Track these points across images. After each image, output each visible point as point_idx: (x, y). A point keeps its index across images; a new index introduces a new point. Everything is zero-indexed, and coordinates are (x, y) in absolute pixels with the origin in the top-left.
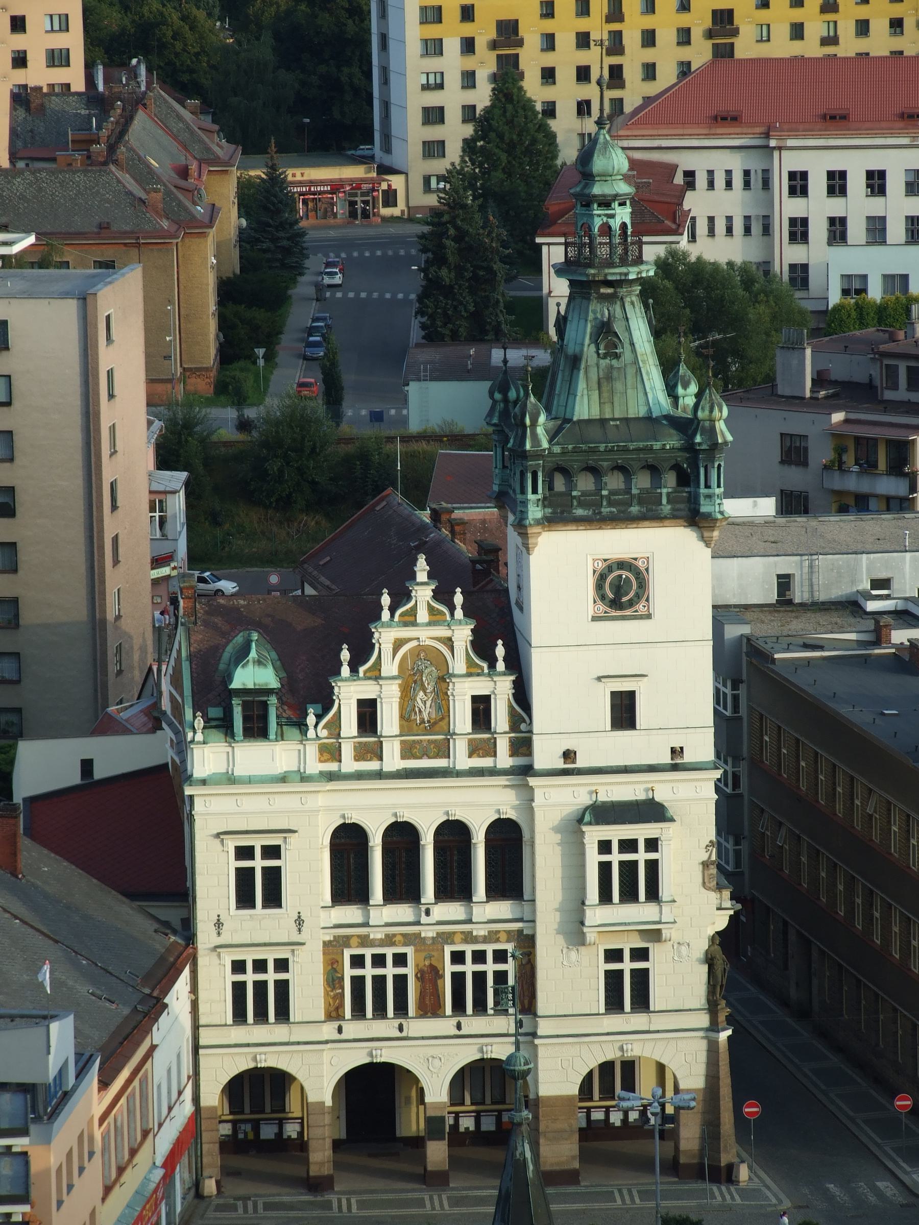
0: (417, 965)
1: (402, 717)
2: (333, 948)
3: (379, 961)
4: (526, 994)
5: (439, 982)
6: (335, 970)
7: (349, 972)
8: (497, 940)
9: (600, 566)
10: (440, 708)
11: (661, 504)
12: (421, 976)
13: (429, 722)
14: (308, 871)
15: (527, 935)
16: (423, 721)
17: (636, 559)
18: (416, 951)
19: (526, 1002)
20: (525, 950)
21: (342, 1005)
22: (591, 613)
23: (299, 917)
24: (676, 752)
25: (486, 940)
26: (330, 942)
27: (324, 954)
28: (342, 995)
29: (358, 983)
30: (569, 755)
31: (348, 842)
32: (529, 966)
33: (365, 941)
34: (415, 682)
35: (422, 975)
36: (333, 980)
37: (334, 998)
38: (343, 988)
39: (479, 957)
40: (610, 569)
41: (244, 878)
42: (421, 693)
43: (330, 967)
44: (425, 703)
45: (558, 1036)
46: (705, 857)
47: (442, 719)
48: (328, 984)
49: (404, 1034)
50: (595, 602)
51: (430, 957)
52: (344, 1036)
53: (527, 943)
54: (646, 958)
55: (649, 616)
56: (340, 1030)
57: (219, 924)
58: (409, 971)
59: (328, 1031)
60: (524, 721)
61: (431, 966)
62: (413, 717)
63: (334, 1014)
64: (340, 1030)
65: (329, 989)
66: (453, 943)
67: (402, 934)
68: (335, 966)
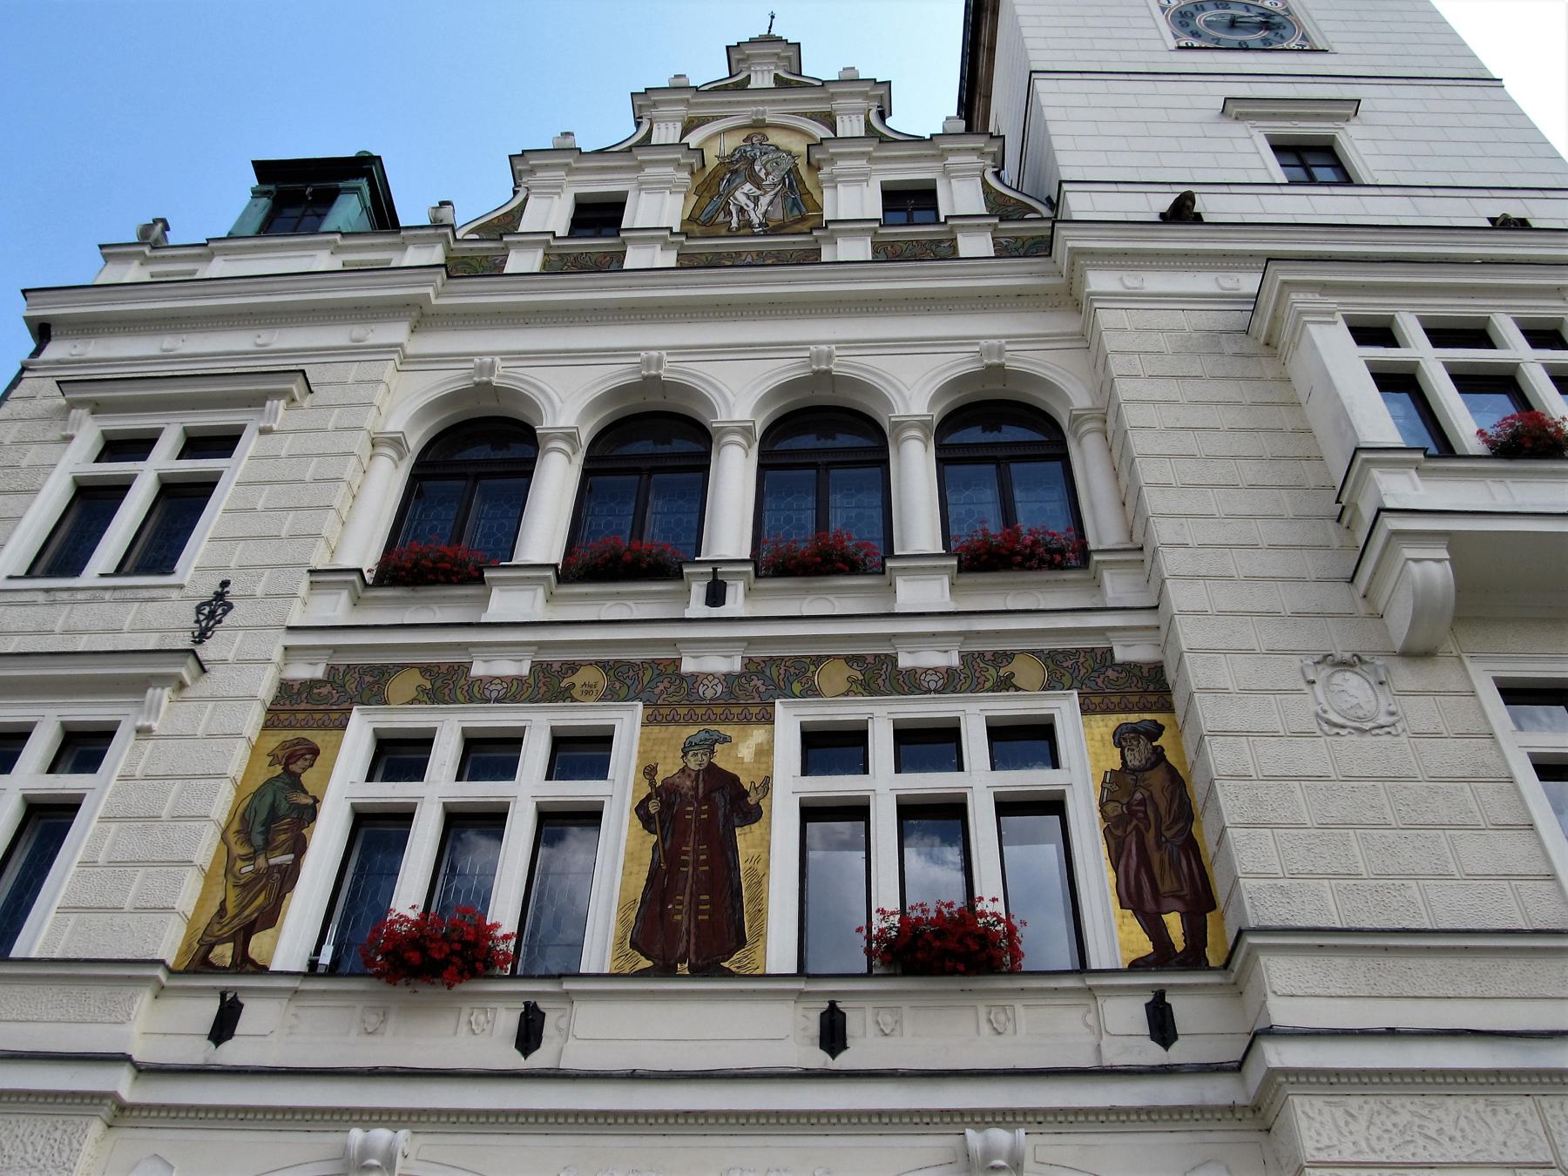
0: (650, 772)
1: (691, 219)
3: (490, 755)
4: (1167, 885)
5: (745, 840)
6: (293, 781)
7: (345, 781)
8: (1006, 684)
10: (795, 204)
12: (662, 810)
13: (761, 225)
14: (316, 496)
15: (1129, 668)
16: (749, 224)
18: (648, 722)
19: (1174, 923)
20: (1133, 718)
21: (270, 917)
22: (1172, 44)
23: (220, 596)
25: (950, 681)
26: (312, 684)
27: (268, 726)
28: (289, 876)
29: (379, 833)
31: (474, 457)
32: (1157, 778)
33: (446, 683)
34: (735, 172)
35: (666, 805)
36: (272, 821)
37: (246, 887)
38: (299, 847)
39: (928, 744)
41: (93, 503)
42: (748, 187)
43: (279, 769)
44: (756, 200)
45: (1391, 1033)
47: (803, 219)
48: (245, 833)
49: (539, 1060)
50: (1176, 37)
51: (710, 743)
52: (232, 1053)
53: (1141, 694)
56: (223, 1028)
58: (616, 793)
59: (169, 1026)
60: (1035, 211)
61: (712, 770)
62: (721, 218)
63: (224, 953)
64: (223, 1028)
65: (240, 850)
66: (812, 691)
67: (603, 665)
68: (293, 768)
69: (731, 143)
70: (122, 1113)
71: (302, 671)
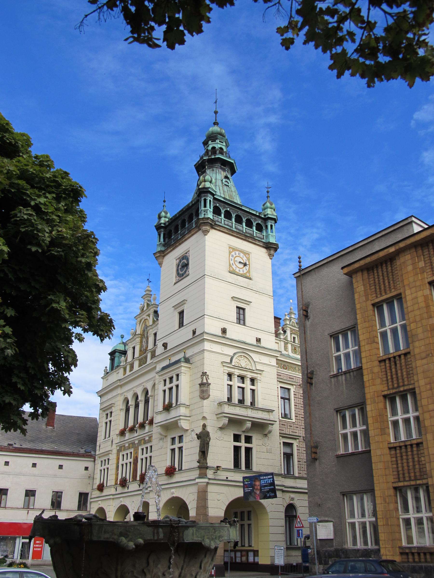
2: (119, 451)
9: (178, 261)
11: (193, 226)
17: (186, 253)
24: (194, 332)
30: (165, 345)
40: (180, 261)
46: (200, 382)
54: (182, 442)
55: (188, 275)
57: (100, 446)
69: (143, 325)
70: (113, 499)
71: (118, 448)
